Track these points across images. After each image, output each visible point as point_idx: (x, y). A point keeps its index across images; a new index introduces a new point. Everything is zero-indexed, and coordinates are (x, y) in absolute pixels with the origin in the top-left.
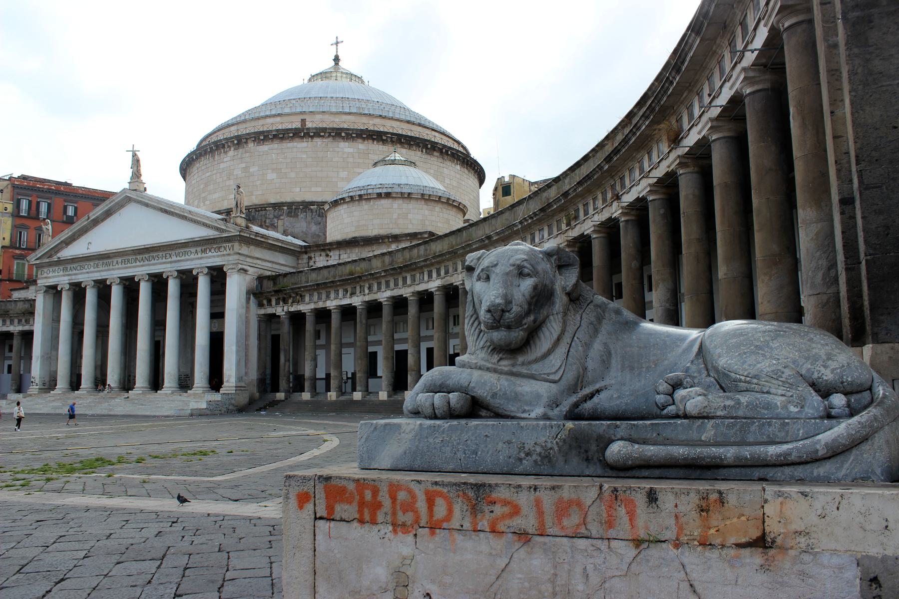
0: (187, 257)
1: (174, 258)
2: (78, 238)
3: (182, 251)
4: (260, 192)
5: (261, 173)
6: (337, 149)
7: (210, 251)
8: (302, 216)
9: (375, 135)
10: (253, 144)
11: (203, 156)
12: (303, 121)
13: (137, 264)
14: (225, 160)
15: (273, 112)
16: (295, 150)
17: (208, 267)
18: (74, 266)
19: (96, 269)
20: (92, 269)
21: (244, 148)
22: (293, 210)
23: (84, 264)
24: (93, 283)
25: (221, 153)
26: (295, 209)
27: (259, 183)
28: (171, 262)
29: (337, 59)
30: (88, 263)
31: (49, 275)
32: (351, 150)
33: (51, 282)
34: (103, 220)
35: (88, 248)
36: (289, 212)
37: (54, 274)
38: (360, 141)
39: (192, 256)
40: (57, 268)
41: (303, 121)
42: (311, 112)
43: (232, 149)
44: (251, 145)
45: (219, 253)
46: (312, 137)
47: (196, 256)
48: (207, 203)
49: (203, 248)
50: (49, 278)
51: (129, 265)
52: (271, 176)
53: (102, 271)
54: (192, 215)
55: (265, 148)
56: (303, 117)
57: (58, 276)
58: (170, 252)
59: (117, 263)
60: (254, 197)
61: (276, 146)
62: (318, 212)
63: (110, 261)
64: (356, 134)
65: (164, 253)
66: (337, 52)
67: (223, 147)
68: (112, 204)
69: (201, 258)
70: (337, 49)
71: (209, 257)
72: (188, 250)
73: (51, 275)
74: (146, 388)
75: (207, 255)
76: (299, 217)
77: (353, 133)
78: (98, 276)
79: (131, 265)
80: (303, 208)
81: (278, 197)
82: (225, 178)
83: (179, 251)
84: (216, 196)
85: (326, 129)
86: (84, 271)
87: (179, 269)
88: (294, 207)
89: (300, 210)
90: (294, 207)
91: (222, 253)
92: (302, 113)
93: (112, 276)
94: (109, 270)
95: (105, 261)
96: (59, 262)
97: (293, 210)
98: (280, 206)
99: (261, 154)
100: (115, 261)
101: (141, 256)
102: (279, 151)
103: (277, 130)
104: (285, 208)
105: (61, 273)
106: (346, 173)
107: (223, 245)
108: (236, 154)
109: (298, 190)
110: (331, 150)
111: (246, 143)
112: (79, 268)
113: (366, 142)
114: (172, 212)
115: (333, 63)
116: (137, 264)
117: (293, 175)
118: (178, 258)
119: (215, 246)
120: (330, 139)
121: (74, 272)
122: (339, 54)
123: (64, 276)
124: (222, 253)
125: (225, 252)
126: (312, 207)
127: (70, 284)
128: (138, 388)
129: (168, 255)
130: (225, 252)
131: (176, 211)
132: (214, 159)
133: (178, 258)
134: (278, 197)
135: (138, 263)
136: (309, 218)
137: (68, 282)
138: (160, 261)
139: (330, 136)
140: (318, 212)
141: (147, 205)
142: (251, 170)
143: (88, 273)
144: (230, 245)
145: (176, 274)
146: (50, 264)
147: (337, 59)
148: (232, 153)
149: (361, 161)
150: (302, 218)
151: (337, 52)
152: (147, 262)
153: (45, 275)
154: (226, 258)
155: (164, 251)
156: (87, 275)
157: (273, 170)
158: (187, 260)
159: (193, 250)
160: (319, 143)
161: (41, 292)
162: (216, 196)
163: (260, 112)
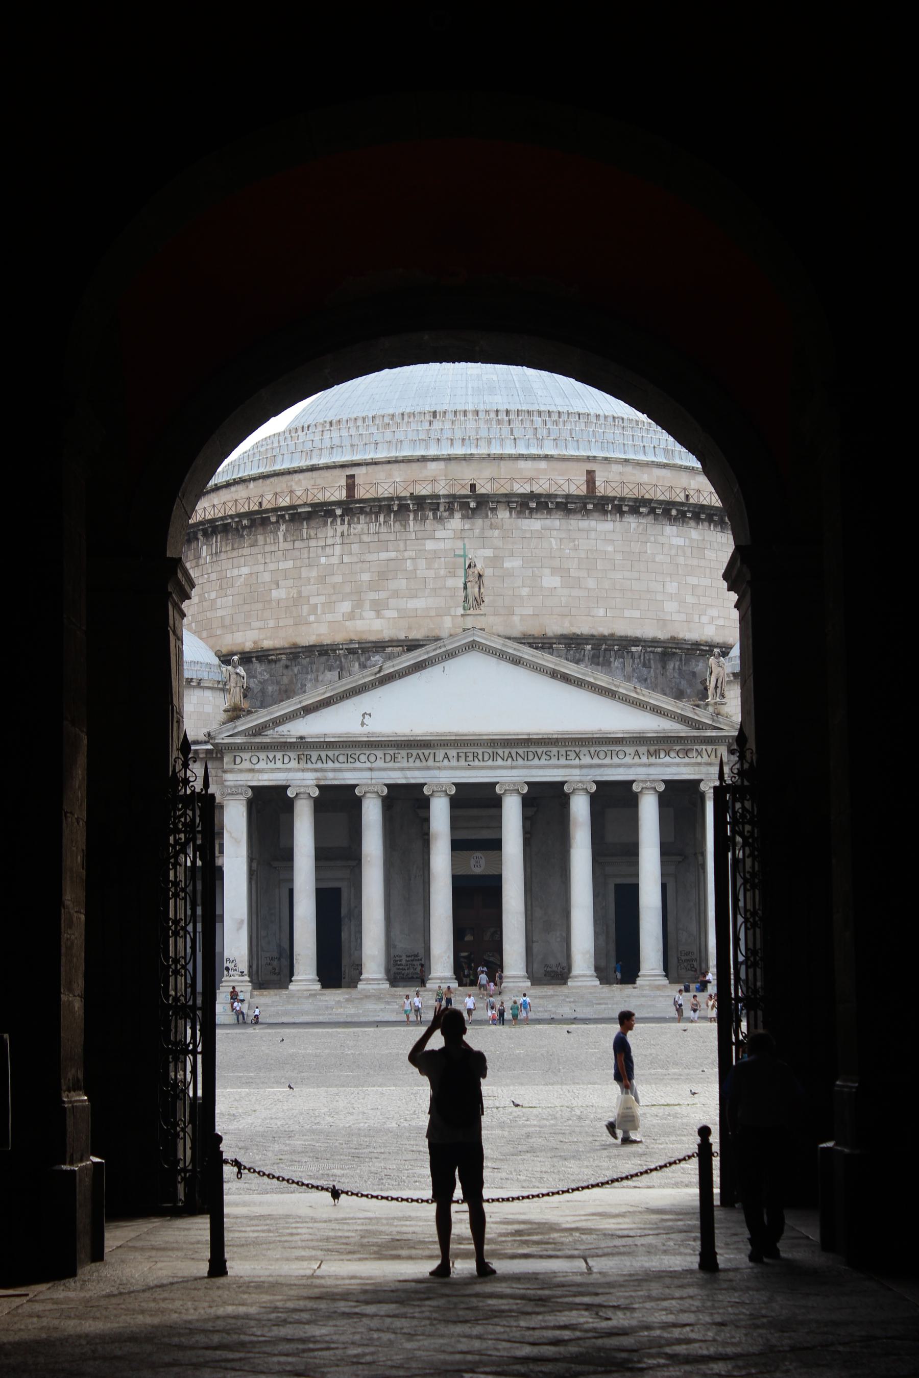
0: (616, 760)
1: (587, 760)
2: (335, 703)
3: (605, 749)
4: (530, 611)
5: (529, 573)
6: (661, 539)
7: (667, 754)
8: (616, 664)
9: (716, 515)
10: (508, 513)
11: (366, 514)
12: (591, 474)
13: (495, 763)
14: (438, 534)
15: (534, 451)
16: (593, 535)
17: (664, 781)
18: (330, 754)
19: (391, 765)
20: (380, 763)
21: (487, 516)
22: (602, 653)
23: (358, 753)
24: (386, 790)
25: (425, 518)
26: (605, 650)
27: (525, 591)
28: (581, 767)
30: (368, 753)
31: (257, 767)
32: (680, 541)
33: (266, 779)
34: (400, 677)
35: (363, 724)
36: (594, 656)
37: (271, 765)
38: (692, 523)
39: (628, 760)
40: (279, 755)
41: (591, 474)
42: (606, 459)
43: (458, 515)
44: (503, 514)
45: (687, 760)
46: (622, 513)
47: (637, 760)
48: (391, 614)
49: (652, 749)
50: (261, 771)
51: (476, 763)
52: (551, 581)
53: (409, 769)
54: (637, 693)
55: (534, 524)
56: (590, 466)
57: (289, 770)
58: (577, 750)
59: (446, 756)
60: (516, 619)
61: (557, 522)
62: (642, 657)
63: (427, 752)
64: (692, 512)
65: (562, 751)
67: (435, 508)
68: (438, 652)
69: (650, 765)
71: (668, 765)
72: (618, 749)
73: (262, 765)
74: (524, 977)
75: (658, 761)
76: (612, 665)
77: (689, 511)
78: (398, 778)
79: (482, 764)
80: (619, 650)
81: (567, 624)
82: (442, 572)
83: (598, 749)
84: (418, 604)
85: (651, 501)
86: (358, 765)
87: (599, 778)
88: (604, 646)
89: (612, 653)
90: (604, 646)
91: (693, 760)
92: (589, 459)
93: (435, 781)
94: (428, 768)
95: (414, 752)
96: (284, 746)
97: (602, 653)
98: (579, 644)
99: (528, 536)
100: (440, 753)
101: (507, 751)
102: (563, 536)
103: (567, 496)
104: (589, 647)
105: (294, 764)
106: (675, 584)
107: (697, 747)
108: (467, 527)
109: (601, 612)
110: (652, 539)
111: (493, 510)
112: (341, 758)
113: (700, 527)
114: (589, 683)
116: (495, 763)
117: (591, 583)
118: (596, 761)
119: (678, 748)
120: (651, 518)
121: (330, 765)
123: (303, 770)
124: (693, 760)
125: (699, 759)
126: (634, 649)
127: (318, 786)
128: (440, 978)
129: (572, 755)
130: (699, 759)
131: (599, 683)
132: (405, 526)
133: (596, 761)
134: (567, 624)
135: (500, 762)
136: (629, 669)
137: (315, 782)
138: (554, 761)
139: (652, 511)
140: (642, 657)
141: (516, 661)
142: (507, 565)
143: (371, 769)
144: (709, 748)
145: (593, 788)
146: (265, 747)
148: (456, 522)
149: (695, 562)
150: (617, 668)
152: (520, 762)
153: (246, 765)
154: (704, 769)
155: (565, 746)
156: (367, 774)
157: (554, 571)
158: (619, 766)
159: (630, 750)
160: (633, 525)
161: (241, 797)
162: (418, 604)
163: (489, 441)
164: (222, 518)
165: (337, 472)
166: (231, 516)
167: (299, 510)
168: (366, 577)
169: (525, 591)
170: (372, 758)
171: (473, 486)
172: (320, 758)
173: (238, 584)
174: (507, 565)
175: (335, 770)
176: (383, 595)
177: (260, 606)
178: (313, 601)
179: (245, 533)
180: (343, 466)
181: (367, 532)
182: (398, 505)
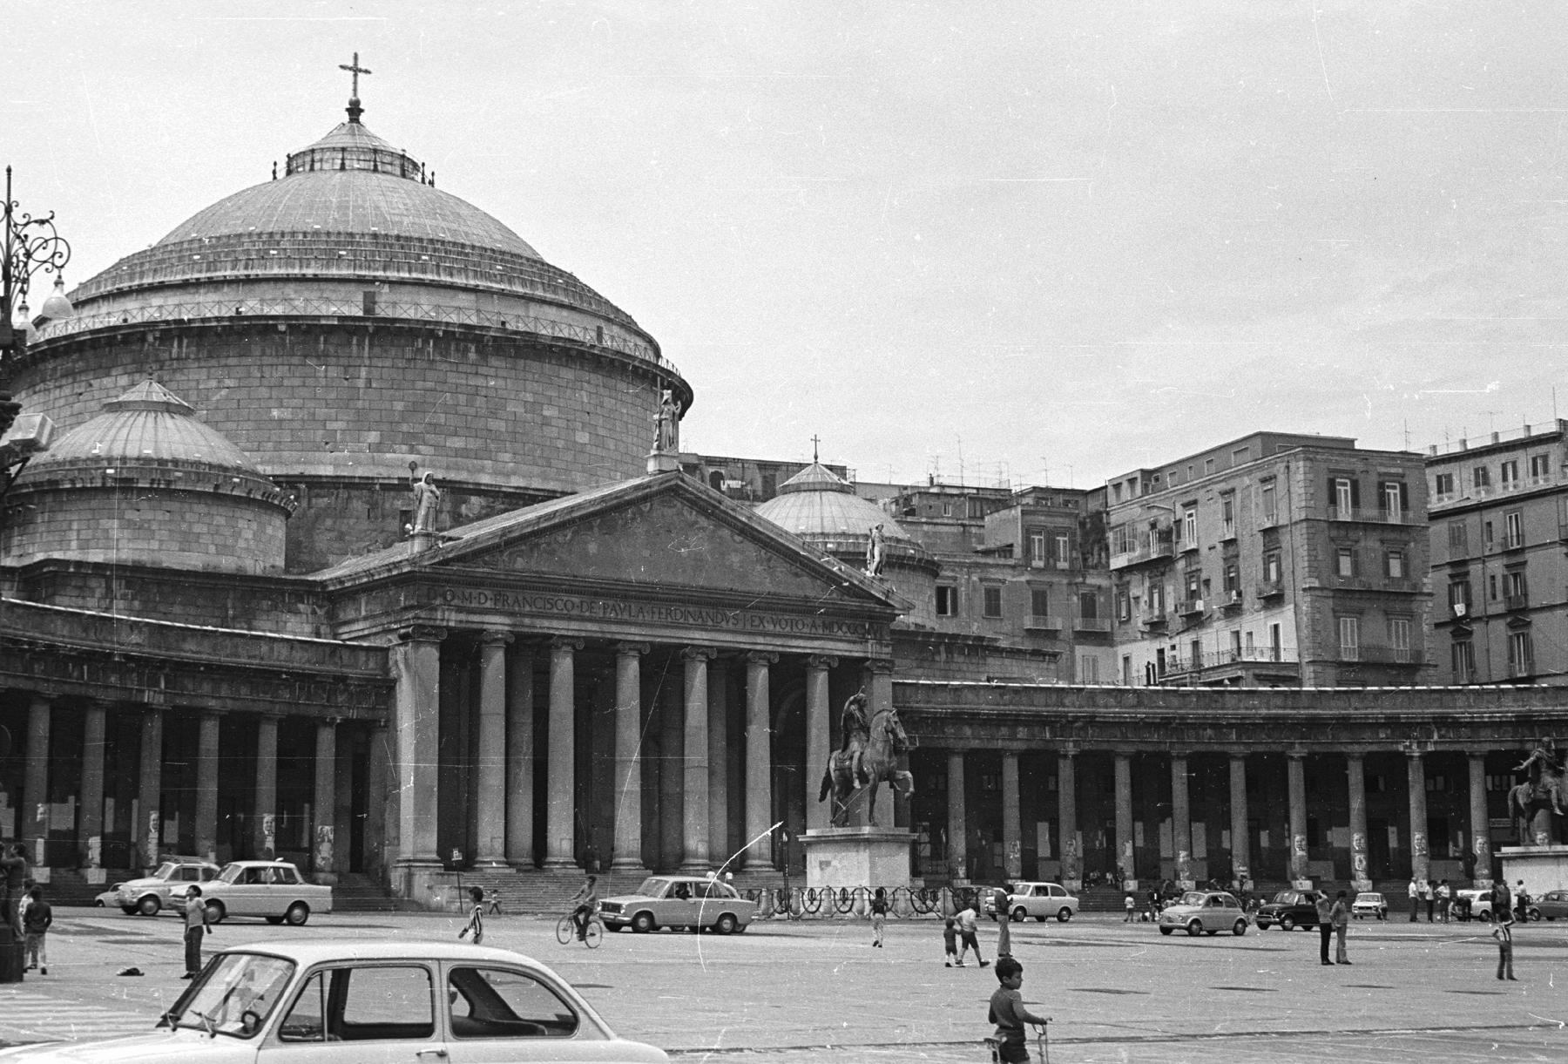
7: (840, 628)
29: (355, 110)
55: (568, 374)
66: (355, 90)
70: (355, 83)
84: (458, 443)
115: (346, 117)
122: (360, 96)
147: (355, 110)
151: (355, 90)
164: (203, 320)
165: (352, 287)
166: (218, 319)
167: (323, 322)
168: (399, 406)
169: (560, 444)
170: (569, 605)
171: (503, 323)
172: (517, 600)
173: (218, 397)
174: (546, 413)
175: (532, 616)
176: (419, 428)
177: (250, 425)
178: (330, 426)
179: (231, 339)
180: (360, 281)
181: (400, 354)
182: (444, 332)
